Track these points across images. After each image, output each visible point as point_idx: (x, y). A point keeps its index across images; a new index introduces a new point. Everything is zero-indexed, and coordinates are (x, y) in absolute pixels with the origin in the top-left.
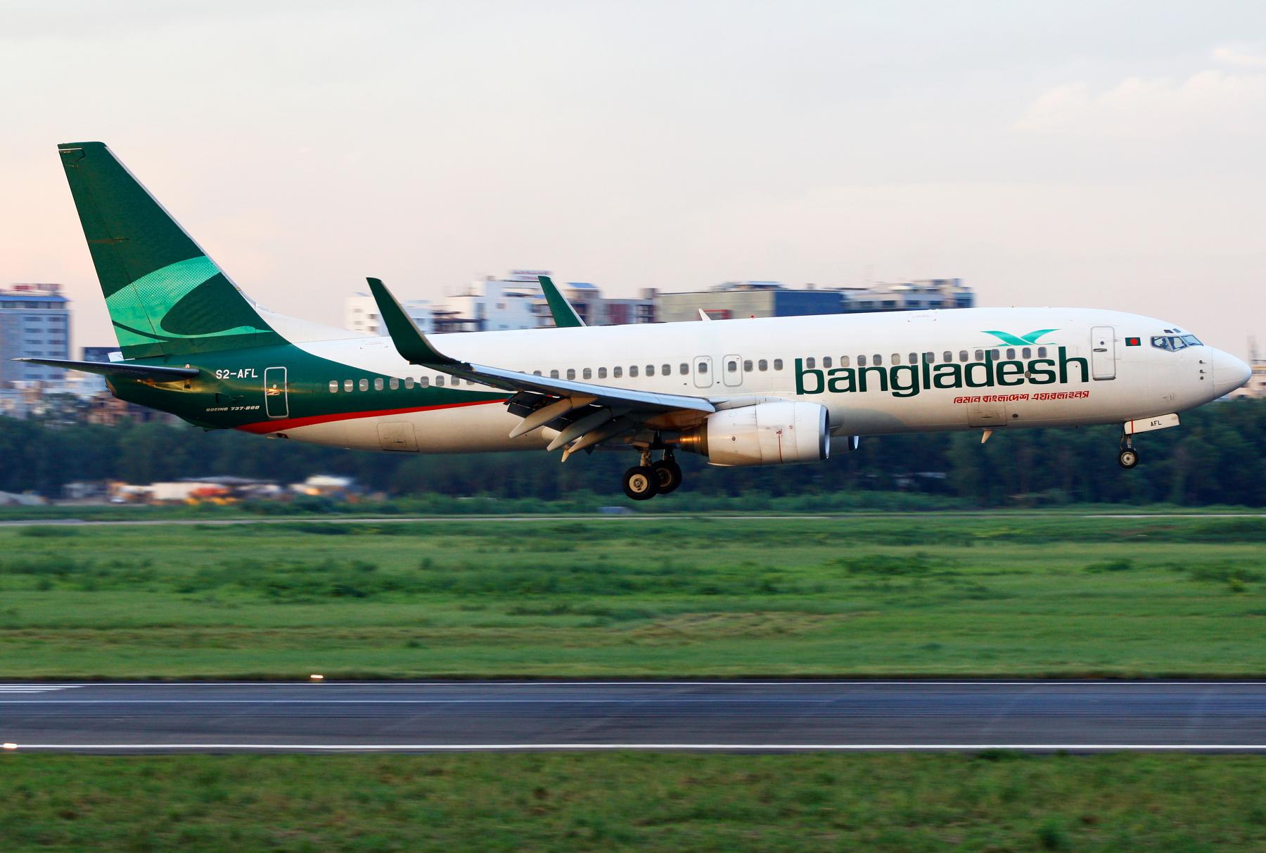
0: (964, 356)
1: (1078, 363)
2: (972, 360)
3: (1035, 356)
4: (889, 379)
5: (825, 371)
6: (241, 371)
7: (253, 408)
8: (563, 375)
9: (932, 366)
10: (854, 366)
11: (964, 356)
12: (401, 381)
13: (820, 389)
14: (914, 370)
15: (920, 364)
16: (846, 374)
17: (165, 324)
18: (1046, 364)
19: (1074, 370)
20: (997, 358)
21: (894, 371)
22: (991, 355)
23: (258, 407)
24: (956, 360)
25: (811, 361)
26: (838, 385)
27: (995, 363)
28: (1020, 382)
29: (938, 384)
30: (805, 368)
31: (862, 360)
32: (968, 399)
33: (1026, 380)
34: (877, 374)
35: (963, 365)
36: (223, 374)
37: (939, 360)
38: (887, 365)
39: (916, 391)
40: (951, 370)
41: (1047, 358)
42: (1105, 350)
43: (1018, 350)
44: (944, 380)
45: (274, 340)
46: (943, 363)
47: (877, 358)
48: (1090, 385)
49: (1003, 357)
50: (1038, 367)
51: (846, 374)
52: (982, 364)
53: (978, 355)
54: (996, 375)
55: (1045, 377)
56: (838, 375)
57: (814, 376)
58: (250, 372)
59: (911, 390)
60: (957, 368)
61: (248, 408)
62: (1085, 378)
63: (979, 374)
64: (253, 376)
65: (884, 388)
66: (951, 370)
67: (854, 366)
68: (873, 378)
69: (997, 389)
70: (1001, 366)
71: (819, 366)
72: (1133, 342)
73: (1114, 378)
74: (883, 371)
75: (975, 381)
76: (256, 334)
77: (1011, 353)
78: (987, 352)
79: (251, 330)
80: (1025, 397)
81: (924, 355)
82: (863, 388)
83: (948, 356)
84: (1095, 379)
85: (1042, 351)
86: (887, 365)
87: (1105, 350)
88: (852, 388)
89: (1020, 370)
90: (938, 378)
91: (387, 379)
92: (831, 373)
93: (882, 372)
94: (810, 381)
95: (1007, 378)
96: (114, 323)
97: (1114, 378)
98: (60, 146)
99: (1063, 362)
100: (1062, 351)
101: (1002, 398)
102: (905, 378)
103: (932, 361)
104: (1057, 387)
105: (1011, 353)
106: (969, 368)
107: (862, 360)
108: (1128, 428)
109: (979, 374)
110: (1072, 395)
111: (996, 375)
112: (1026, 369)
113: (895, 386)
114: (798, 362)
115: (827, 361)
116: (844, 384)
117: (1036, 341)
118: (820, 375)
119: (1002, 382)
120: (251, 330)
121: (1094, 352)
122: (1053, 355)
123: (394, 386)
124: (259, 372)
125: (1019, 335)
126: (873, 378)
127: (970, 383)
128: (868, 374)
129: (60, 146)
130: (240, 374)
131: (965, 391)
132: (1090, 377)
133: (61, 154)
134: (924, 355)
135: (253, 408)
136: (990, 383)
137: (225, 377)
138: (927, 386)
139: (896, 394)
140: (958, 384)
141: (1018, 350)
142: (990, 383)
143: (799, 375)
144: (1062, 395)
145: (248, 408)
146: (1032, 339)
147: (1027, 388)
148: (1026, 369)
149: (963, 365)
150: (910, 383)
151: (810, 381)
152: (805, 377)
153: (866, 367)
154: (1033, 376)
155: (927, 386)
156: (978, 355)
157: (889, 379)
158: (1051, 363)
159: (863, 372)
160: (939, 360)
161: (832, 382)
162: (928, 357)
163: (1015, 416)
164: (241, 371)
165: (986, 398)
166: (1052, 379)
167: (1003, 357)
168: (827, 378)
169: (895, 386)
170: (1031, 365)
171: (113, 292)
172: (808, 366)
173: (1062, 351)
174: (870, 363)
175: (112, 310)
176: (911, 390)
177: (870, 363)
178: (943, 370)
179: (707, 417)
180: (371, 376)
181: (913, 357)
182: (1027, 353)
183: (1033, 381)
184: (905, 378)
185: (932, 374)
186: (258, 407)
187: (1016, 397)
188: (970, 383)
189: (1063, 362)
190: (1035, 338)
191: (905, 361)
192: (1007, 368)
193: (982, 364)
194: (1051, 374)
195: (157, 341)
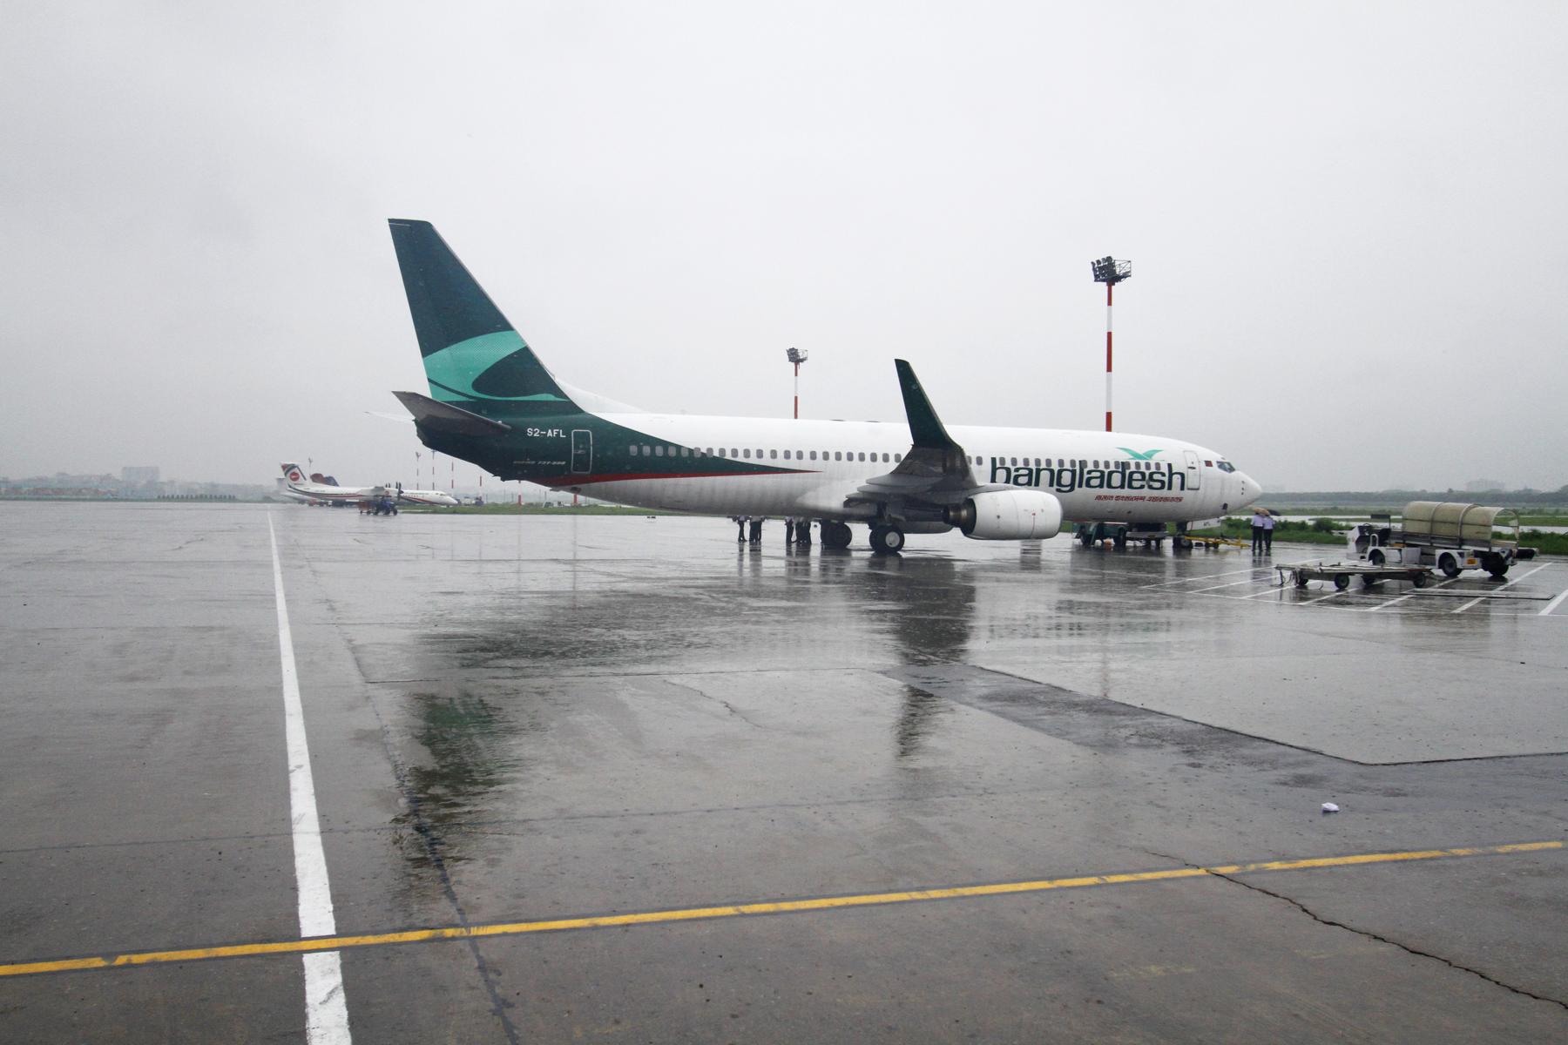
0: (1107, 464)
1: (1179, 476)
2: (1112, 468)
3: (1153, 469)
5: (1013, 468)
6: (550, 431)
7: (559, 463)
8: (781, 454)
9: (1086, 471)
10: (1032, 466)
11: (1107, 464)
12: (691, 451)
14: (1073, 472)
15: (1077, 468)
16: (1026, 472)
17: (477, 385)
18: (1160, 475)
19: (1176, 479)
20: (1129, 468)
21: (1060, 472)
22: (1125, 465)
23: (564, 463)
24: (1102, 467)
25: (1003, 460)
26: (1021, 480)
27: (1128, 472)
28: (1142, 487)
29: (1088, 485)
30: (998, 465)
31: (1038, 462)
32: (1105, 497)
33: (1146, 486)
34: (1048, 473)
35: (1106, 471)
36: (534, 433)
37: (1090, 467)
38: (1055, 467)
39: (1072, 489)
40: (1098, 474)
41: (1161, 471)
42: (1194, 468)
43: (1143, 463)
44: (1095, 482)
45: (571, 408)
46: (1093, 469)
47: (1049, 462)
48: (1186, 494)
49: (1133, 468)
50: (1156, 477)
51: (1026, 472)
52: (1118, 472)
53: (1117, 464)
54: (1127, 481)
55: (1157, 485)
56: (1021, 472)
57: (1004, 472)
58: (559, 432)
59: (1068, 488)
60: (1102, 472)
61: (554, 463)
62: (1182, 488)
64: (561, 436)
65: (1051, 485)
66: (1098, 474)
67: (1032, 466)
68: (1045, 476)
69: (1126, 492)
71: (1008, 464)
72: (1208, 464)
73: (1198, 489)
76: (555, 402)
77: (1138, 465)
78: (1123, 463)
79: (551, 398)
80: (1142, 498)
81: (1080, 462)
82: (1037, 484)
83: (1096, 463)
84: (1189, 489)
85: (1158, 466)
86: (1055, 467)
87: (1194, 468)
88: (1029, 483)
89: (1143, 478)
90: (1089, 480)
91: (679, 447)
92: (1017, 470)
93: (1052, 471)
94: (1001, 474)
95: (1135, 484)
96: (430, 380)
97: (1198, 489)
98: (390, 221)
99: (1171, 474)
100: (1170, 466)
101: (1128, 498)
103: (1086, 467)
104: (1165, 493)
105: (1138, 465)
106: (1110, 473)
107: (1038, 462)
108: (1189, 527)
110: (1173, 499)
111: (1127, 481)
112: (1147, 477)
113: (1059, 484)
114: (994, 460)
115: (1014, 461)
117: (1153, 457)
118: (1008, 470)
119: (1130, 486)
120: (551, 398)
121: (1190, 470)
122: (1165, 469)
123: (685, 454)
124: (567, 433)
125: (1141, 452)
126: (1045, 476)
127: (1109, 486)
128: (1042, 472)
129: (390, 221)
130: (550, 433)
131: (1105, 491)
132: (1185, 487)
133: (390, 226)
134: (1080, 462)
135: (559, 463)
136: (1122, 486)
137: (535, 435)
138: (1080, 486)
139: (1058, 490)
140: (1101, 486)
141: (1143, 463)
142: (1122, 486)
143: (994, 469)
144: (1166, 499)
145: (554, 463)
146: (1150, 455)
147: (1146, 492)
148: (1147, 477)
149: (1106, 471)
151: (1001, 474)
152: (998, 471)
153: (1041, 467)
154: (1151, 483)
155: (1080, 486)
156: (1117, 464)
158: (1163, 475)
159: (1038, 471)
160: (1090, 467)
161: (1016, 477)
162: (1083, 464)
163: (1129, 512)
164: (550, 431)
165: (1118, 498)
166: (1162, 487)
167: (1133, 468)
168: (1013, 474)
170: (1151, 474)
171: (428, 354)
172: (1001, 464)
173: (1170, 466)
174: (1043, 465)
175: (428, 370)
176: (1068, 488)
177: (1043, 465)
178: (1094, 474)
179: (972, 497)
180: (666, 444)
181: (1073, 463)
182: (1148, 466)
183: (1151, 487)
185: (1086, 476)
186: (564, 463)
187: (1137, 498)
188: (1109, 486)
189: (1171, 474)
190: (1152, 455)
191: (1067, 466)
192: (1137, 476)
193: (1118, 472)
194: (1163, 482)
195: (467, 399)
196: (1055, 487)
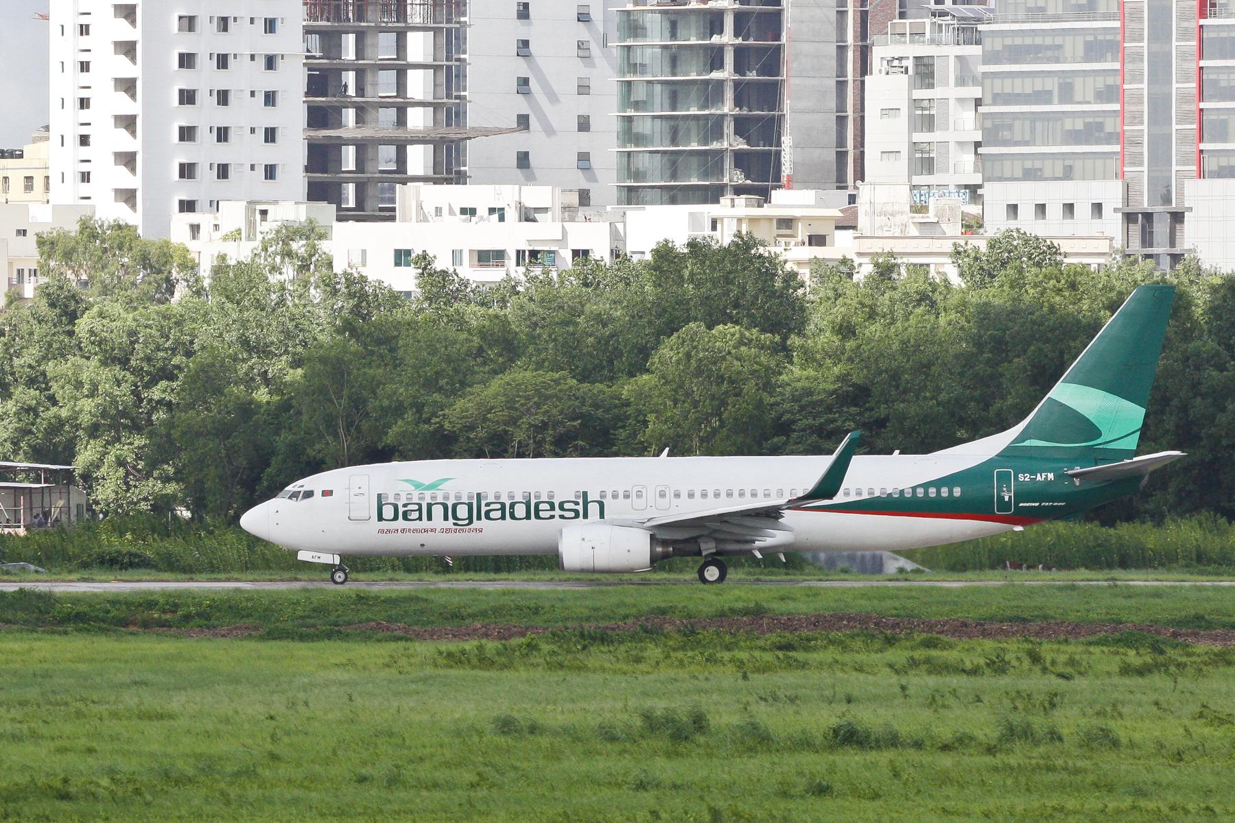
4: (450, 512)
9: (483, 503)
13: (396, 518)
14: (470, 506)
19: (593, 509)
28: (552, 517)
29: (488, 517)
39: (471, 522)
44: (493, 515)
55: (572, 514)
59: (467, 522)
63: (520, 511)
65: (446, 518)
68: (438, 511)
70: (537, 505)
74: (446, 507)
75: (517, 515)
82: (430, 518)
88: (420, 518)
89: (553, 508)
94: (388, 512)
95: (542, 514)
102: (462, 512)
106: (512, 506)
109: (520, 511)
113: (455, 517)
116: (415, 515)
119: (538, 517)
126: (438, 511)
127: (513, 517)
136: (528, 517)
138: (479, 518)
139: (455, 524)
150: (466, 516)
151: (388, 512)
155: (479, 518)
157: (450, 512)
159: (430, 506)
166: (577, 516)
168: (401, 510)
169: (455, 517)
183: (562, 517)
184: (462, 512)
185: (484, 509)
192: (542, 507)
194: (577, 512)
196: (451, 520)
